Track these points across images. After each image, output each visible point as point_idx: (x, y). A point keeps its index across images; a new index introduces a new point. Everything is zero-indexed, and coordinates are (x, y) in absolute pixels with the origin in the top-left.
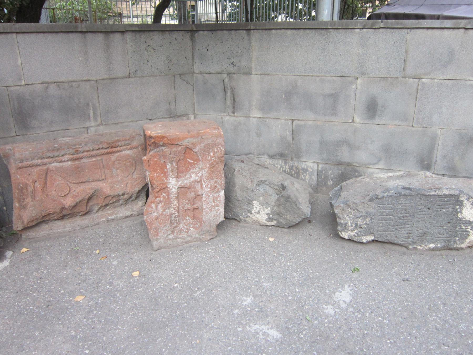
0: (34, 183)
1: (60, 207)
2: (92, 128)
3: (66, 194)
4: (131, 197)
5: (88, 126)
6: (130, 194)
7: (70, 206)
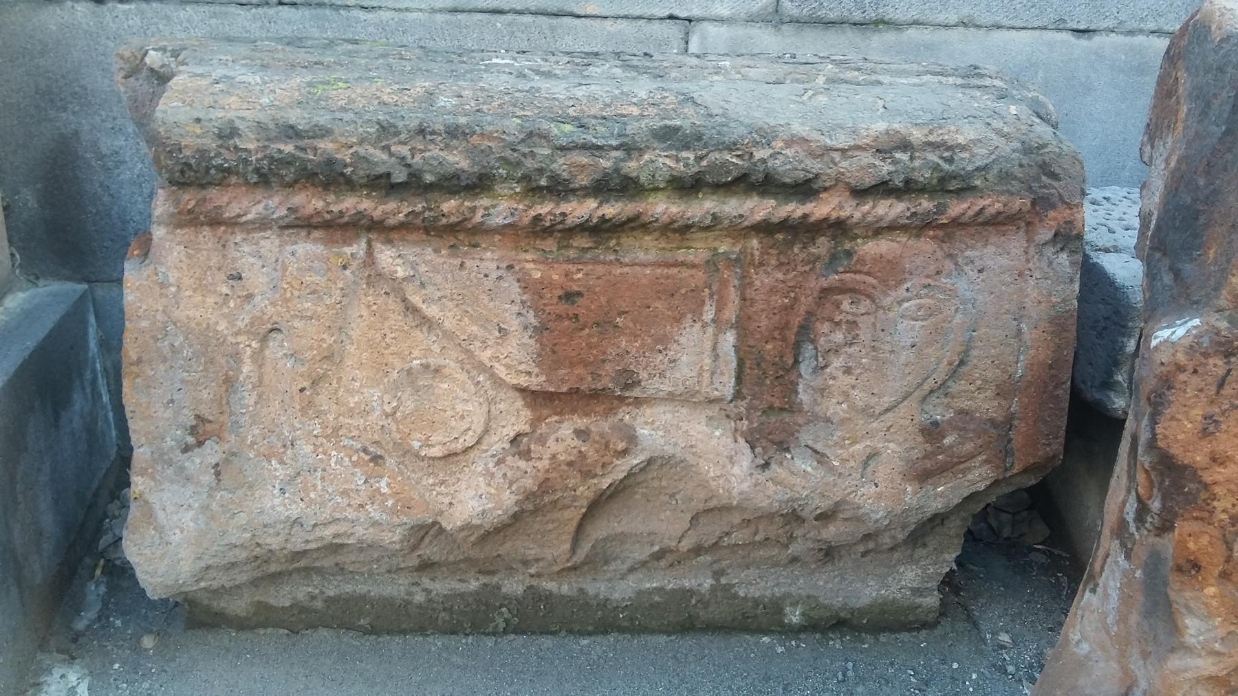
0: (264, 340)
1: (409, 519)
2: (712, 29)
3: (459, 446)
5: (696, 12)
6: (870, 527)
7: (467, 527)
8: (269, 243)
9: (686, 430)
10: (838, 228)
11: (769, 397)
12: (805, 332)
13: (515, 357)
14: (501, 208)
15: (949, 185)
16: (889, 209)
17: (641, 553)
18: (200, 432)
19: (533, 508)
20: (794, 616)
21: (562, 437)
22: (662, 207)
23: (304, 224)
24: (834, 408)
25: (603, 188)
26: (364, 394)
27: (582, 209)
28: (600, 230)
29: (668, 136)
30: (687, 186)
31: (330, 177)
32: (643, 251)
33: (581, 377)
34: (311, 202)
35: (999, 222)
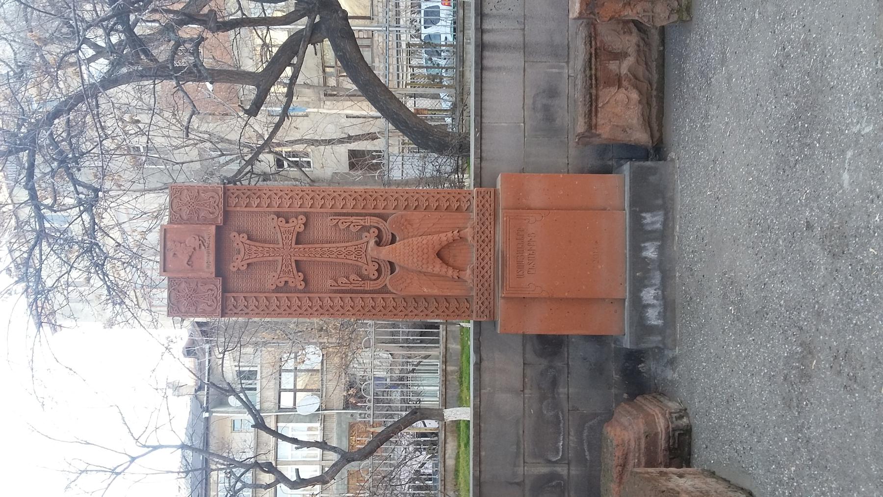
4: (643, 39)
8: (599, 120)
9: (625, 67)
10: (596, 49)
11: (619, 56)
12: (610, 52)
13: (613, 90)
14: (594, 91)
15: (590, 37)
16: (593, 43)
17: (647, 73)
18: (624, 131)
19: (636, 87)
20: (662, 48)
21: (625, 83)
22: (593, 72)
23: (596, 115)
24: (621, 47)
25: (591, 80)
26: (618, 110)
27: (594, 82)
28: (596, 80)
29: (584, 72)
30: (591, 69)
31: (590, 111)
32: (599, 74)
33: (618, 82)
34: (593, 114)
35: (595, 29)
